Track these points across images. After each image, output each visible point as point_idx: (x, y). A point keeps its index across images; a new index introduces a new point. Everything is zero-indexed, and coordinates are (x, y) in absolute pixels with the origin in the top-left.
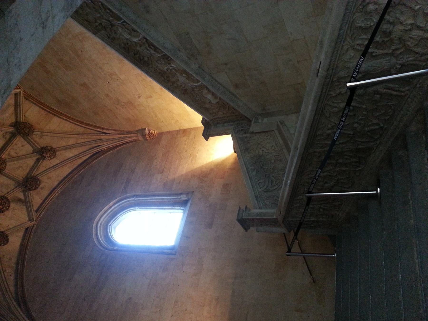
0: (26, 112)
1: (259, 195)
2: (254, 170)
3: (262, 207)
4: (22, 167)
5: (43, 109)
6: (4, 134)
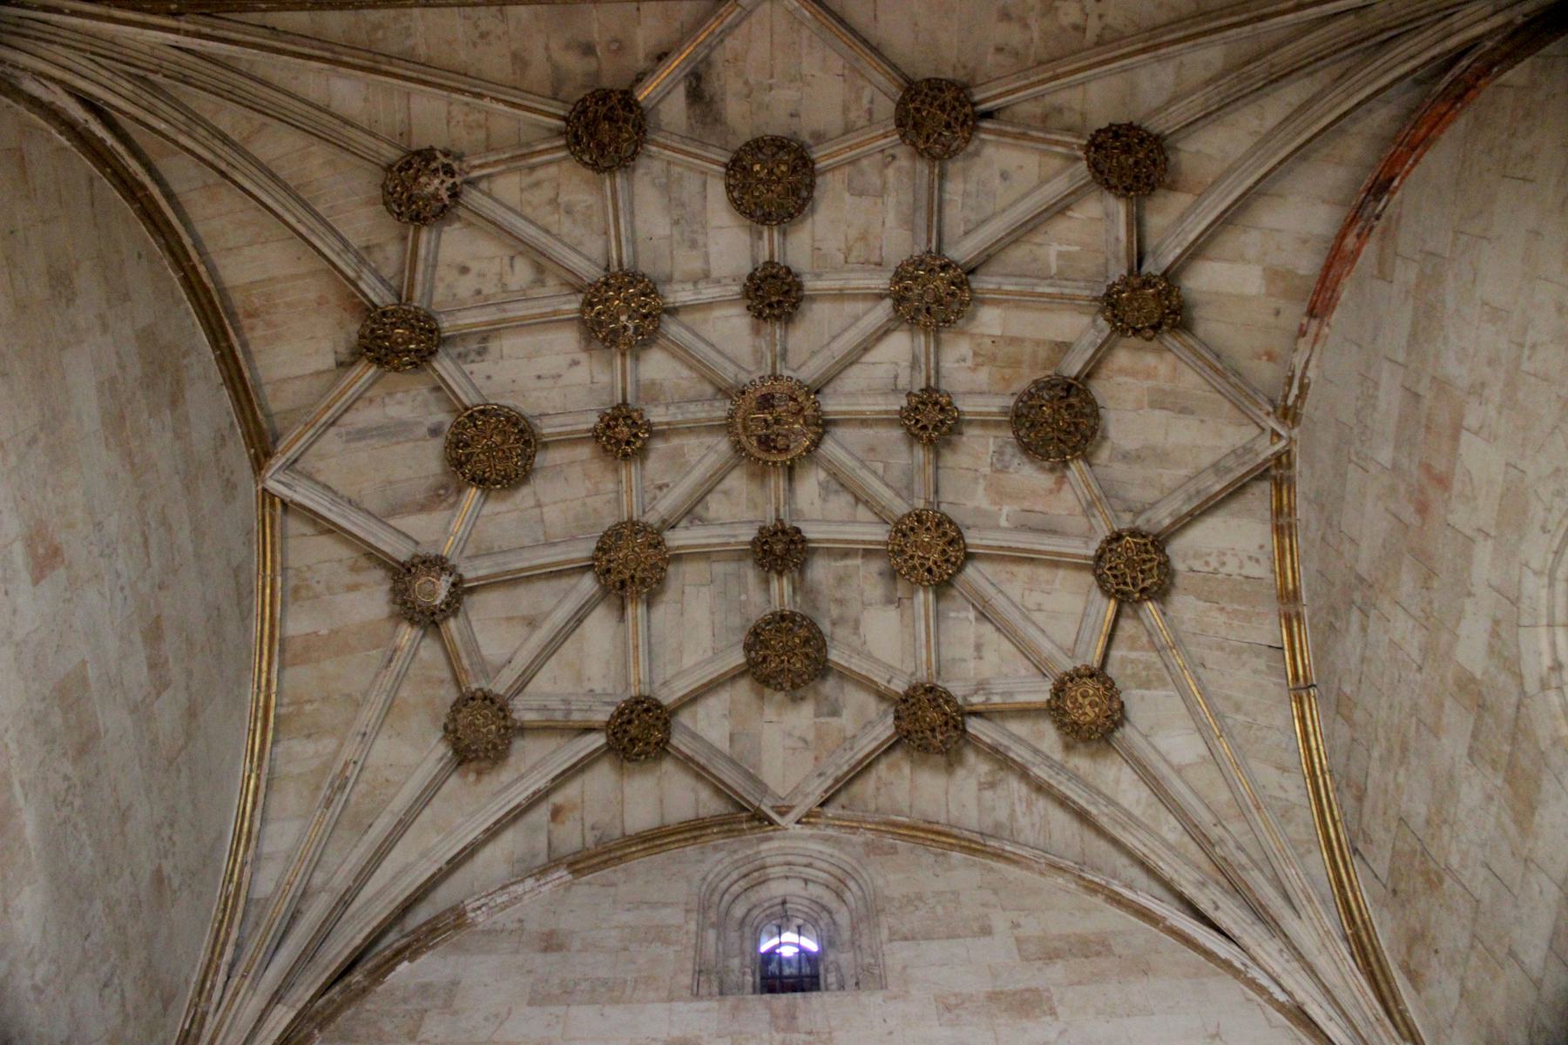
0: (318, 373)
4: (554, 202)
5: (245, 345)
6: (473, 356)
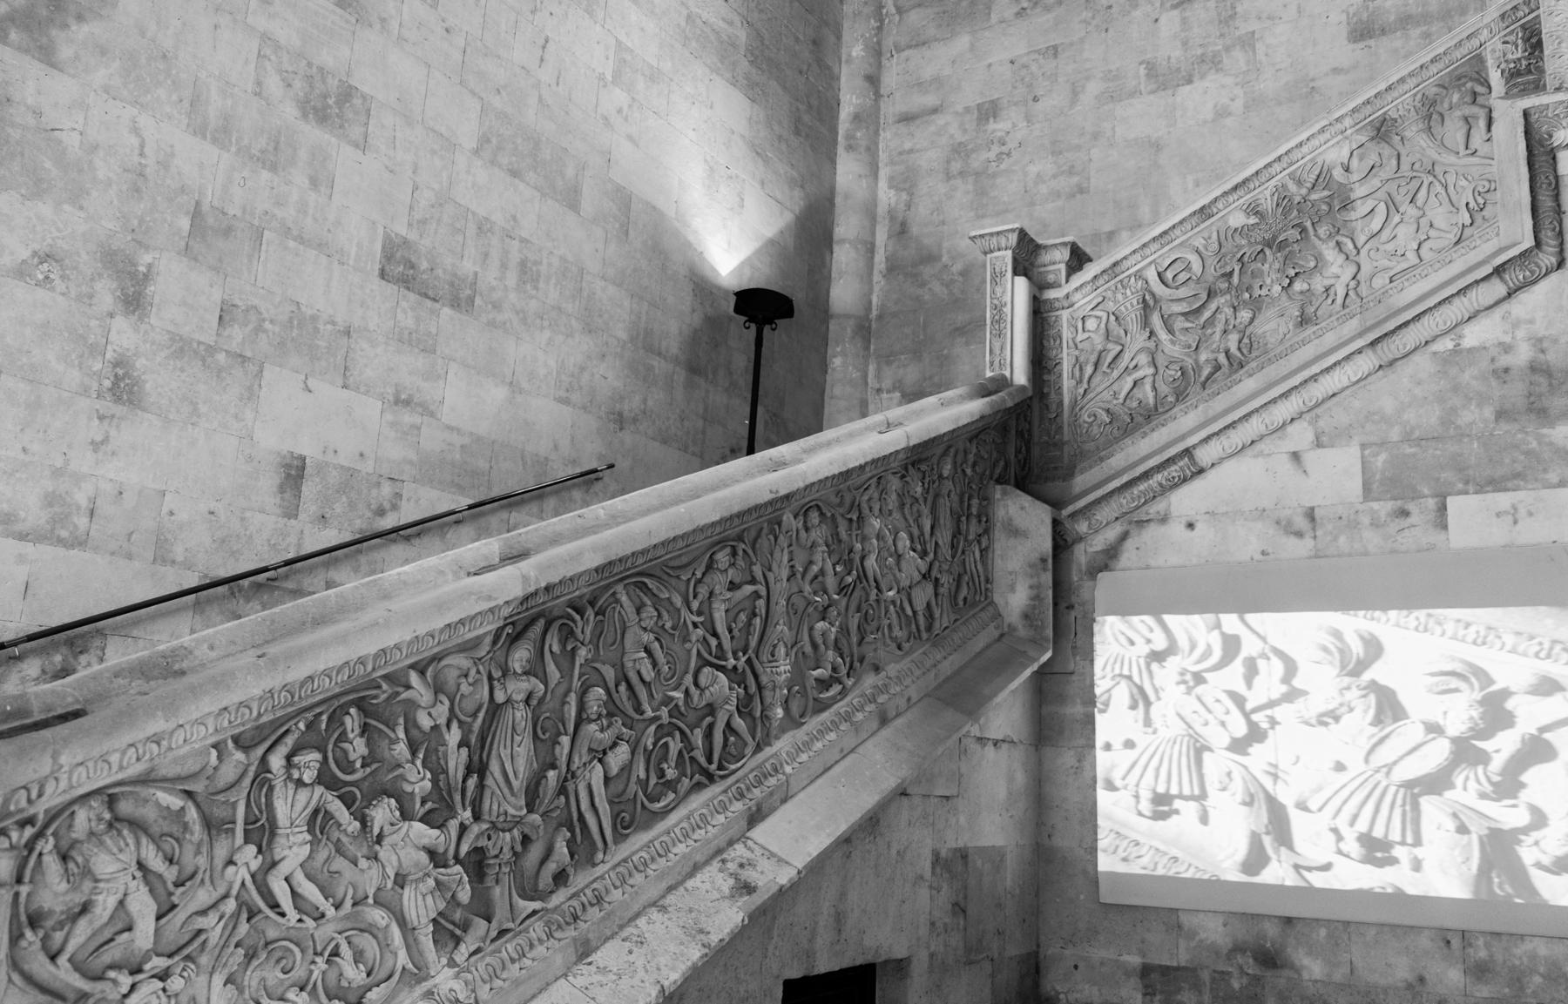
1: (1129, 277)
2: (1254, 210)
3: (1076, 306)
